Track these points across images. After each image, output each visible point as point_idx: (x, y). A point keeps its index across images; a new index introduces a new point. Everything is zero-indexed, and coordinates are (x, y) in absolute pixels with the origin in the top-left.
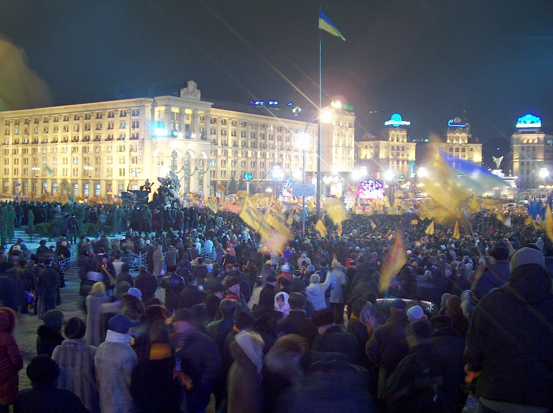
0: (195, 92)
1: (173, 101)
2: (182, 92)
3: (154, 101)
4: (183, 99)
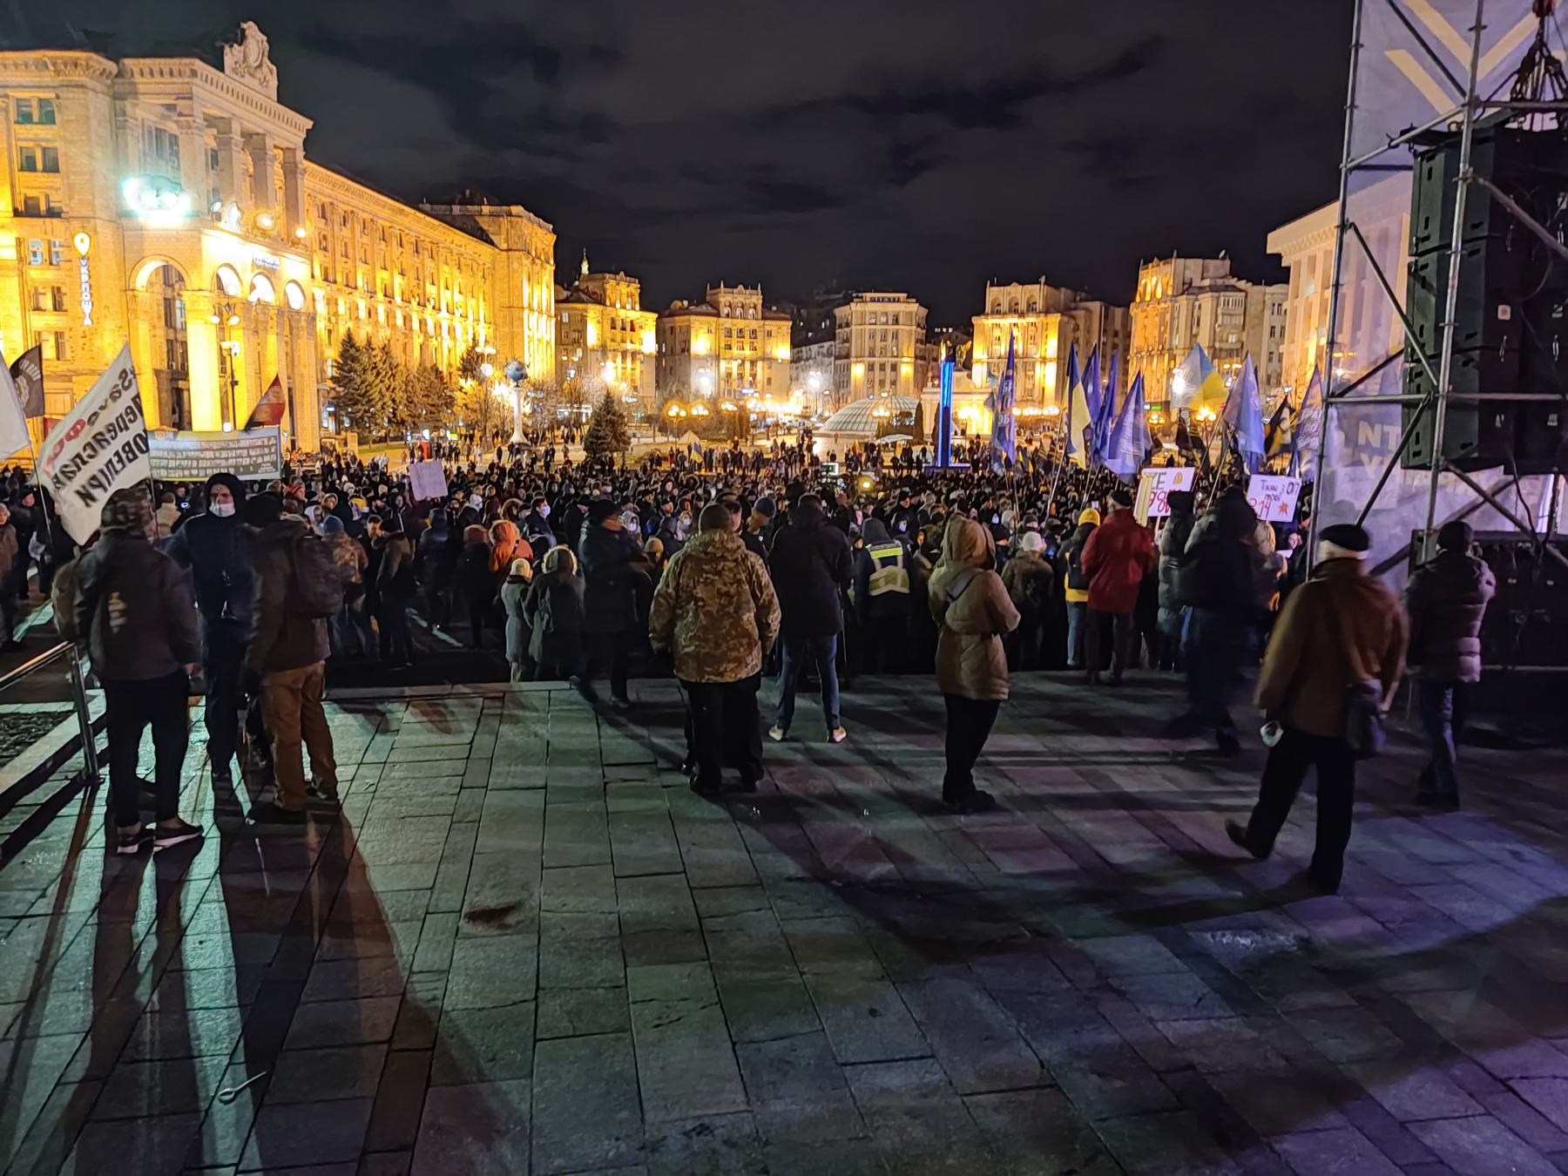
0: (265, 69)
1: (208, 86)
2: (231, 55)
3: (120, 74)
4: (227, 82)
